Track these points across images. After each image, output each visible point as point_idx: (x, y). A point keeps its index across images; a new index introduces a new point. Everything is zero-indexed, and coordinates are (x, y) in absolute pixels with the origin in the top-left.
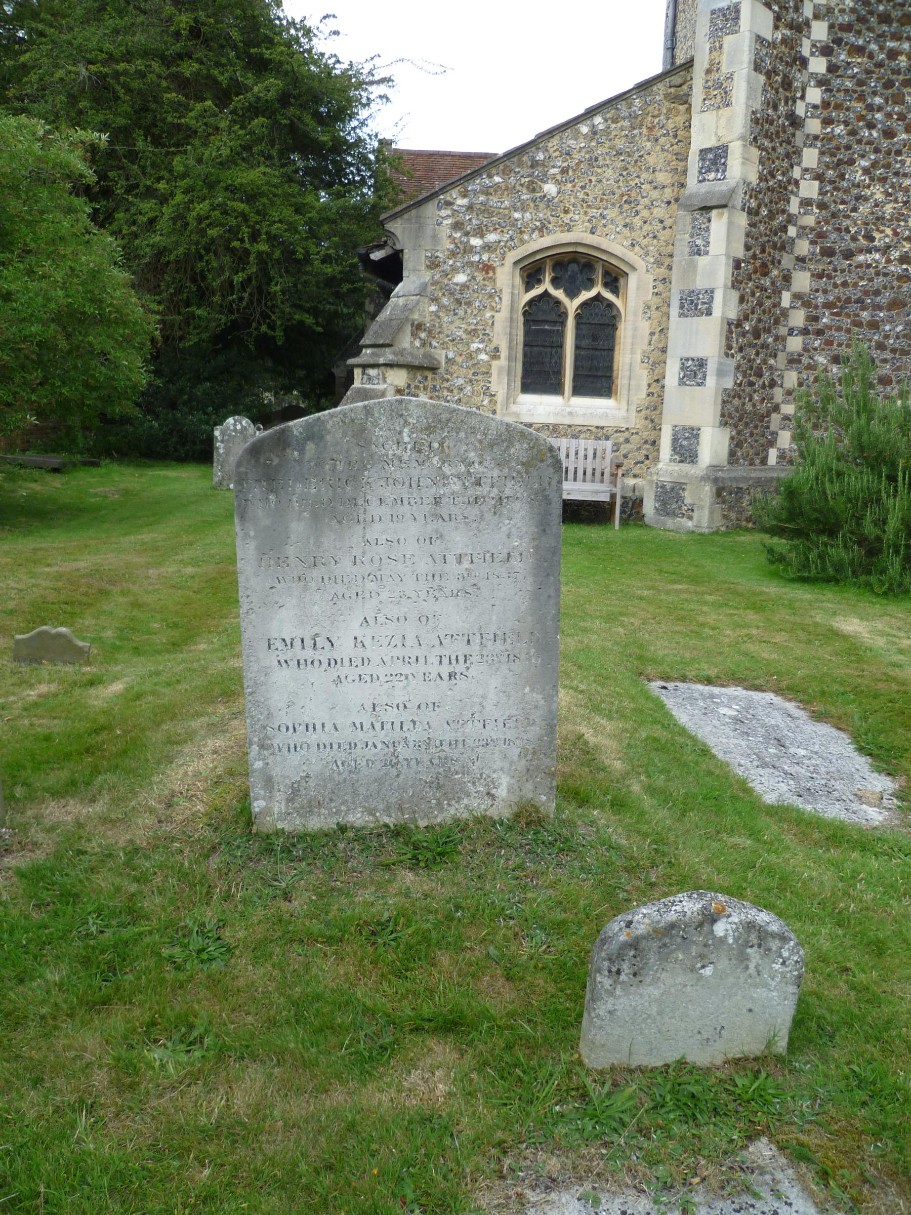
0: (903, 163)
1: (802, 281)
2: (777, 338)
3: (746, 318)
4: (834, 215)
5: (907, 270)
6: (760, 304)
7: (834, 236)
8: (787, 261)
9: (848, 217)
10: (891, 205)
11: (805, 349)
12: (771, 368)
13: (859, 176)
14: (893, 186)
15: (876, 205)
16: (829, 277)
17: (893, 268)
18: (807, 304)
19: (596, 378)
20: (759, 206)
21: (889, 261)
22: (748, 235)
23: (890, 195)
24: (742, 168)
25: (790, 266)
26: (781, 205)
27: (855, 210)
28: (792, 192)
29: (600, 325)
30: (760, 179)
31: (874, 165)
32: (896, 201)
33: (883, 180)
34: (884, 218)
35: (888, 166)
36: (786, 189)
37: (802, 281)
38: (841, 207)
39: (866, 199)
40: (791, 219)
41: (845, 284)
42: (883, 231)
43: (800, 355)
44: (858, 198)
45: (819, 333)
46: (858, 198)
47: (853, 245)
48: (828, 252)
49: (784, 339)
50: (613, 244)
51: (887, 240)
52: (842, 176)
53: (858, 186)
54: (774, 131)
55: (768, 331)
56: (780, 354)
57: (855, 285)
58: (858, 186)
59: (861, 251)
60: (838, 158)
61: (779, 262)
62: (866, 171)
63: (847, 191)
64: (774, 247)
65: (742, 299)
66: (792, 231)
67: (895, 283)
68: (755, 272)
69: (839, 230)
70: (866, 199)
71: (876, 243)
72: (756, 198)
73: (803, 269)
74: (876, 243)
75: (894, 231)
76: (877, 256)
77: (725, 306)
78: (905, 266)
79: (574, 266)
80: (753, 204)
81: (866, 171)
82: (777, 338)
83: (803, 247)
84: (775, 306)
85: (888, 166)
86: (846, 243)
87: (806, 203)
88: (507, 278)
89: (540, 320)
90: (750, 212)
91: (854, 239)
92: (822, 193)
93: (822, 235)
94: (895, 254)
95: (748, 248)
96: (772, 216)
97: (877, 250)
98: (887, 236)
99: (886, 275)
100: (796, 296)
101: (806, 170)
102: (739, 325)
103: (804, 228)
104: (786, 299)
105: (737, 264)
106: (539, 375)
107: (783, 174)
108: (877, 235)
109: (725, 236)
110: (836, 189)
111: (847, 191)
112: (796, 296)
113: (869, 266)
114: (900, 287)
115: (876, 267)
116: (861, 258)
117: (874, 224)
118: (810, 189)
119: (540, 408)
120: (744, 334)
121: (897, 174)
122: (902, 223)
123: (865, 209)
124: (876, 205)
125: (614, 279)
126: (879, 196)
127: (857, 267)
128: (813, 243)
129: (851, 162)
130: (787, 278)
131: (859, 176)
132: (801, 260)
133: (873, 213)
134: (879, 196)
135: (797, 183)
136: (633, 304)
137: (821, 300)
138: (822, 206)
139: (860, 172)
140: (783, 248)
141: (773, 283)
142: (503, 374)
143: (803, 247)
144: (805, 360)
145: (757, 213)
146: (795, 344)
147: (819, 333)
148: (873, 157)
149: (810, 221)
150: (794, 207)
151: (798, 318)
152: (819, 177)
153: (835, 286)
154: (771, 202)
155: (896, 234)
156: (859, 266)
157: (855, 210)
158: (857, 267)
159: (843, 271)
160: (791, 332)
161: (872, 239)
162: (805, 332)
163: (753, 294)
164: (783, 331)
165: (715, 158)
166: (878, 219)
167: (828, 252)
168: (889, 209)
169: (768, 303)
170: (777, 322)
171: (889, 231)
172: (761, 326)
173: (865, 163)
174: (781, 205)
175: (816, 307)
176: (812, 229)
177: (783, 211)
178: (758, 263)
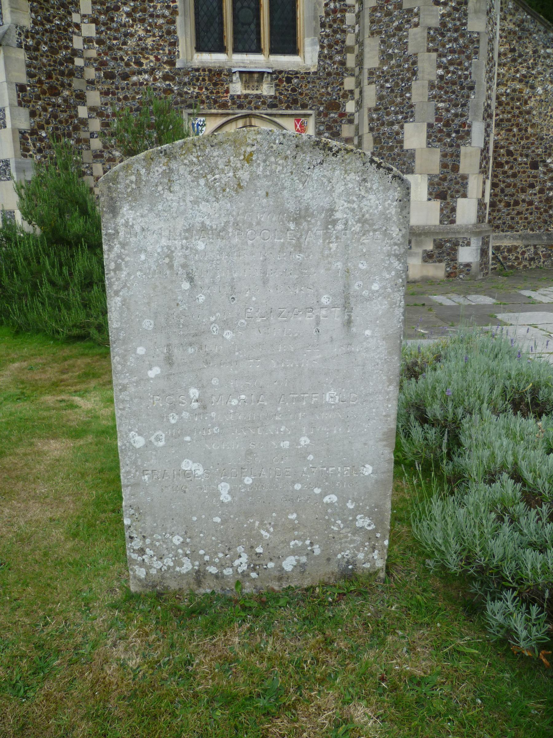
0: (155, 7)
1: (94, 98)
2: (78, 141)
3: (42, 127)
4: (110, 48)
5: (169, 85)
6: (55, 117)
7: (112, 64)
8: (77, 84)
9: (120, 49)
10: (151, 39)
11: (105, 147)
12: (77, 162)
13: (124, 19)
14: (150, 25)
15: (140, 39)
16: (114, 94)
17: (159, 84)
18: (100, 114)
20: (38, 44)
21: (155, 79)
22: (28, 66)
23: (150, 31)
25: (83, 87)
26: (63, 42)
27: (125, 43)
28: (73, 33)
30: (35, 23)
31: (134, 9)
32: (154, 36)
33: (142, 21)
34: (147, 49)
35: (144, 10)
36: (66, 30)
37: (94, 98)
38: (115, 42)
39: (132, 35)
40: (76, 53)
41: (126, 98)
42: (147, 58)
43: (101, 151)
44: (126, 35)
45: (113, 135)
46: (126, 35)
47: (127, 70)
48: (110, 76)
49: (87, 141)
51: (152, 64)
52: (112, 20)
53: (125, 26)
55: (69, 136)
56: (85, 152)
57: (134, 98)
58: (125, 26)
59: (134, 73)
61: (70, 85)
62: (129, 15)
63: (117, 30)
64: (62, 73)
65: (33, 114)
66: (79, 62)
67: (163, 95)
68: (44, 93)
69: (115, 59)
70: (132, 35)
71: (144, 67)
72: (33, 38)
73: (94, 89)
74: (144, 67)
75: (156, 57)
76: (146, 76)
78: (167, 83)
80: (30, 42)
81: (129, 15)
82: (78, 141)
83: (91, 73)
84: (71, 117)
85: (144, 10)
86: (122, 68)
87: (87, 40)
90: (27, 48)
91: (128, 65)
92: (98, 32)
93: (103, 64)
94: (159, 74)
95: (30, 75)
96: (53, 51)
97: (146, 72)
98: (151, 61)
99: (155, 89)
100: (92, 109)
101: (84, 16)
102: (33, 132)
103: (89, 59)
104: (83, 112)
105: (21, 88)
107: (61, 19)
108: (144, 61)
110: (109, 29)
111: (117, 30)
112: (92, 109)
113: (141, 84)
114: (166, 98)
115: (147, 84)
116: (135, 78)
117: (140, 53)
118: (89, 30)
120: (41, 140)
121: (152, 16)
122: (161, 52)
123: (131, 42)
124: (140, 39)
126: (141, 33)
127: (132, 85)
128: (97, 69)
129: (117, 8)
130: (81, 98)
131: (124, 19)
132: (91, 83)
133: (138, 45)
134: (141, 33)
135: (78, 26)
137: (110, 111)
138: (100, 42)
139: (125, 16)
140: (71, 74)
141: (65, 100)
143: (91, 73)
144: (106, 155)
145: (37, 49)
146: (96, 144)
147: (113, 135)
148: (132, 4)
149: (93, 53)
150: (77, 43)
151: (96, 125)
152: (95, 21)
153: (119, 100)
154: (51, 40)
155: (157, 59)
156: (134, 84)
157: (125, 43)
158: (132, 85)
159: (123, 89)
160: (92, 135)
161: (141, 64)
162: (102, 134)
163: (45, 110)
164: (84, 135)
166: (143, 49)
167: (110, 76)
168: (149, 42)
169: (63, 116)
170: (76, 128)
171: (152, 58)
172: (59, 132)
173: (127, 9)
174: (63, 42)
175: (108, 116)
176: (96, 60)
177: (67, 48)
178: (45, 87)
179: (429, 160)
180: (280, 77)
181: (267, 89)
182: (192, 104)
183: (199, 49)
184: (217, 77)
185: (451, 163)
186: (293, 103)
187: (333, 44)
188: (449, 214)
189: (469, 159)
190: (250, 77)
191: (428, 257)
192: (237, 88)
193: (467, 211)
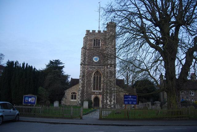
19: (75, 99)
24: (81, 89)
29: (75, 96)
37: (85, 93)
50: (76, 92)
54: (83, 87)
60: (87, 87)
77: (80, 95)
79: (74, 93)
88: (70, 94)
89: (72, 96)
106: (72, 99)
109: (80, 92)
118: (86, 89)
119: (72, 100)
125: (76, 94)
136: (77, 95)
142: (70, 99)
165: (80, 88)
179: (109, 99)
180: (99, 92)
181: (98, 93)
182: (93, 94)
183: (93, 90)
184: (94, 92)
185: (111, 99)
186: (100, 94)
187: (103, 89)
188: (111, 103)
189: (112, 99)
190: (97, 92)
191: (109, 106)
192: (96, 93)
193: (112, 103)
